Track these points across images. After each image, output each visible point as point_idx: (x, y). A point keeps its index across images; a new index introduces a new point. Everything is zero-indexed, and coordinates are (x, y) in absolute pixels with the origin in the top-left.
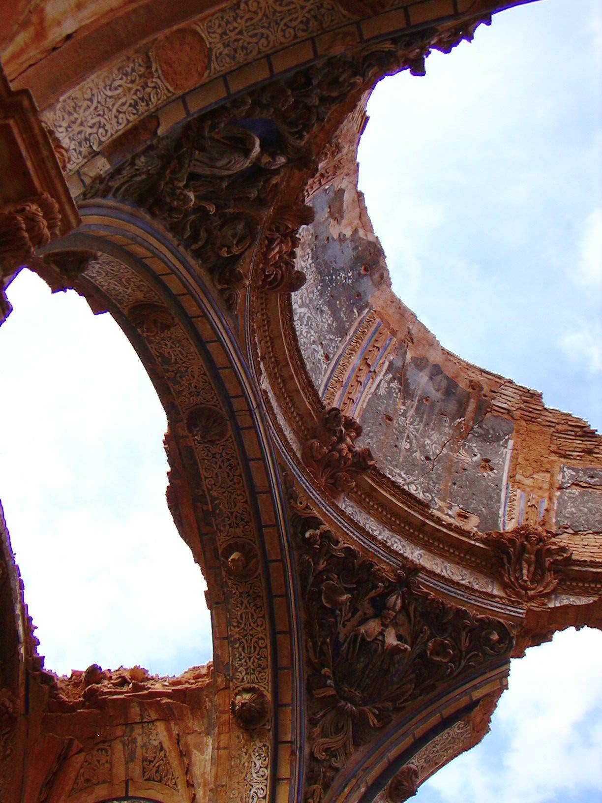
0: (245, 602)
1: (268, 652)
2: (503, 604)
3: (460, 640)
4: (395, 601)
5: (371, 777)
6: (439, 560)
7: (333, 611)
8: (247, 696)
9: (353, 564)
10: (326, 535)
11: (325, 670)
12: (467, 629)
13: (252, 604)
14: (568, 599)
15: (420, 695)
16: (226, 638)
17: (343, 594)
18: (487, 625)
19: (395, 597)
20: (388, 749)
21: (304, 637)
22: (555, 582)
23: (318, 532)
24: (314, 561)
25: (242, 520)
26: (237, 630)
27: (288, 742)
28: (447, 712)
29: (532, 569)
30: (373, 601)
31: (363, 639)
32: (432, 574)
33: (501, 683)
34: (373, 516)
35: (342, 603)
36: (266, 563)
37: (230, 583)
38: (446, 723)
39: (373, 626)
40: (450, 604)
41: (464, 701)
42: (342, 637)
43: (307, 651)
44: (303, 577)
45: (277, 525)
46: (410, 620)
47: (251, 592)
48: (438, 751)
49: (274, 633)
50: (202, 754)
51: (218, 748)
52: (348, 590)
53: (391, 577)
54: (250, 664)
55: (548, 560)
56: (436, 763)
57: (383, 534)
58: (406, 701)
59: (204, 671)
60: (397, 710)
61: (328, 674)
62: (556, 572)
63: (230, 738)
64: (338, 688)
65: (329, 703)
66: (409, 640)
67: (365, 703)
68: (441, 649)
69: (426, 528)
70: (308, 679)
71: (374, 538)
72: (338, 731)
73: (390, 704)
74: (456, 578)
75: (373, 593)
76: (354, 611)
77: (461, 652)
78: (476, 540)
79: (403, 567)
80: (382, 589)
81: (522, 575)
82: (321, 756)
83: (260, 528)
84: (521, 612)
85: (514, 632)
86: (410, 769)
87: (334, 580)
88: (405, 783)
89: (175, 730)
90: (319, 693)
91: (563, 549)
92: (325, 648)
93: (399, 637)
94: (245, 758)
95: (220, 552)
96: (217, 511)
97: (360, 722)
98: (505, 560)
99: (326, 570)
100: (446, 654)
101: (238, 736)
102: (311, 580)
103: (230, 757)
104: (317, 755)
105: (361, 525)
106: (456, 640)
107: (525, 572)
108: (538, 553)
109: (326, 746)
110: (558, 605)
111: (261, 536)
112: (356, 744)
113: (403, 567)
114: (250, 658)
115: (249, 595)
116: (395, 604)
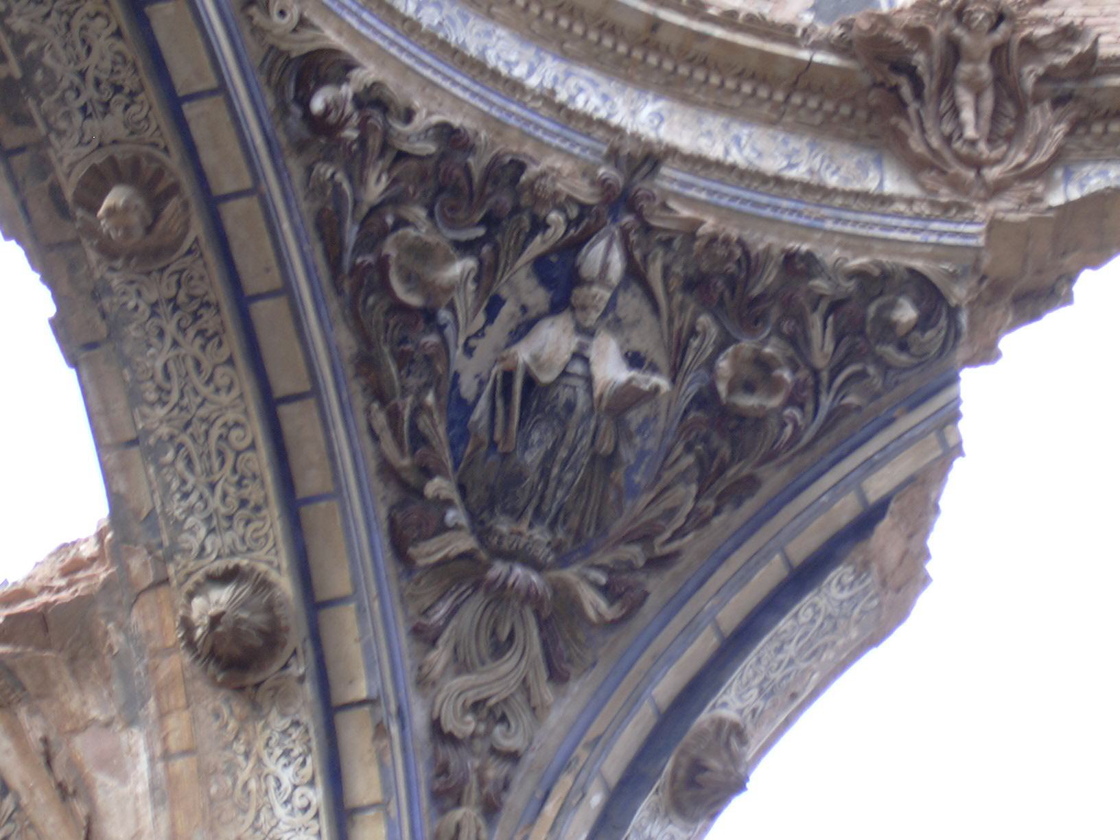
0: (171, 328)
1: (262, 460)
2: (918, 217)
3: (808, 341)
4: (604, 257)
5: (613, 765)
6: (714, 123)
7: (428, 316)
8: (222, 597)
9: (467, 169)
10: (373, 101)
11: (438, 486)
12: (823, 306)
13: (191, 333)
14: (1104, 173)
15: (717, 512)
16: (134, 442)
17: (449, 260)
18: (877, 283)
19: (601, 246)
20: (650, 678)
21: (359, 402)
22: (1060, 130)
23: (347, 90)
24: (350, 178)
25: (118, 89)
26: (161, 412)
27: (362, 703)
28: (802, 547)
29: (988, 102)
30: (541, 266)
31: (530, 382)
32: (699, 163)
33: (943, 442)
34: (506, 24)
35: (450, 288)
36: (212, 204)
37: (116, 281)
38: (804, 577)
39: (552, 341)
40: (764, 241)
41: (846, 510)
42: (468, 387)
43: (375, 438)
44: (327, 229)
45: (222, 89)
47: (182, 298)
48: (791, 662)
49: (270, 405)
50: (124, 779)
51: (167, 756)
52: (465, 248)
53: (585, 192)
54: (215, 502)
55: (1030, 73)
56: (794, 696)
57: (539, 70)
58: (679, 533)
59: (88, 550)
60: (658, 563)
62: (1058, 102)
63: (194, 720)
64: (481, 531)
65: (462, 573)
66: (660, 358)
67: (564, 561)
68: (759, 373)
69: (663, 36)
70: (392, 521)
71: (515, 87)
72: (499, 649)
74: (772, 164)
75: (537, 246)
76: (494, 306)
77: (816, 373)
78: (815, 46)
79: (613, 156)
81: (960, 126)
82: (466, 725)
83: (175, 103)
84: (970, 231)
85: (959, 293)
86: (720, 724)
87: (421, 224)
88: (714, 763)
89: (35, 730)
90: (429, 552)
91: (1069, 33)
92: (423, 422)
93: (634, 360)
94: (246, 771)
95: (69, 194)
96: (39, 76)
97: (557, 616)
98: (906, 91)
99: (393, 200)
100: (775, 386)
101: (215, 709)
102: (351, 233)
103: (204, 775)
104: (449, 725)
105: (472, 51)
106: (798, 342)
107: (967, 115)
108: (999, 54)
109: (471, 696)
110: (1075, 194)
111: (182, 126)
112: (557, 676)
113: (613, 156)
114: (212, 487)
115: (176, 308)
116: (605, 266)
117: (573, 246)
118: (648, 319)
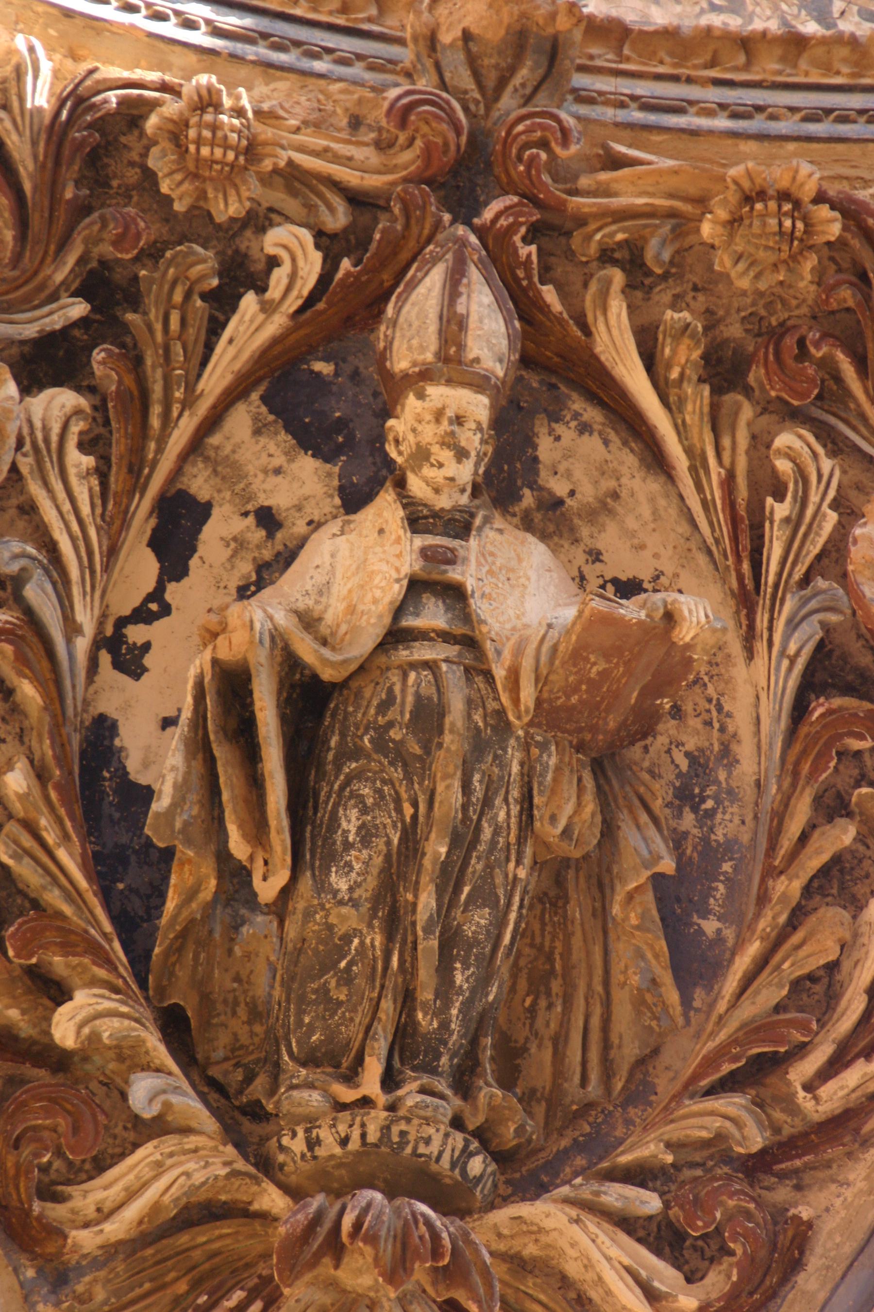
19: (430, 286)
31: (290, 664)
39: (356, 568)
46: (656, 459)
53: (361, 166)
61: (109, 1029)
64: (245, 1120)
73: (733, 1104)
75: (252, 328)
80: (312, 264)
116: (452, 327)
117: (349, 310)
118: (640, 486)
